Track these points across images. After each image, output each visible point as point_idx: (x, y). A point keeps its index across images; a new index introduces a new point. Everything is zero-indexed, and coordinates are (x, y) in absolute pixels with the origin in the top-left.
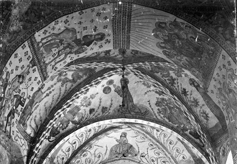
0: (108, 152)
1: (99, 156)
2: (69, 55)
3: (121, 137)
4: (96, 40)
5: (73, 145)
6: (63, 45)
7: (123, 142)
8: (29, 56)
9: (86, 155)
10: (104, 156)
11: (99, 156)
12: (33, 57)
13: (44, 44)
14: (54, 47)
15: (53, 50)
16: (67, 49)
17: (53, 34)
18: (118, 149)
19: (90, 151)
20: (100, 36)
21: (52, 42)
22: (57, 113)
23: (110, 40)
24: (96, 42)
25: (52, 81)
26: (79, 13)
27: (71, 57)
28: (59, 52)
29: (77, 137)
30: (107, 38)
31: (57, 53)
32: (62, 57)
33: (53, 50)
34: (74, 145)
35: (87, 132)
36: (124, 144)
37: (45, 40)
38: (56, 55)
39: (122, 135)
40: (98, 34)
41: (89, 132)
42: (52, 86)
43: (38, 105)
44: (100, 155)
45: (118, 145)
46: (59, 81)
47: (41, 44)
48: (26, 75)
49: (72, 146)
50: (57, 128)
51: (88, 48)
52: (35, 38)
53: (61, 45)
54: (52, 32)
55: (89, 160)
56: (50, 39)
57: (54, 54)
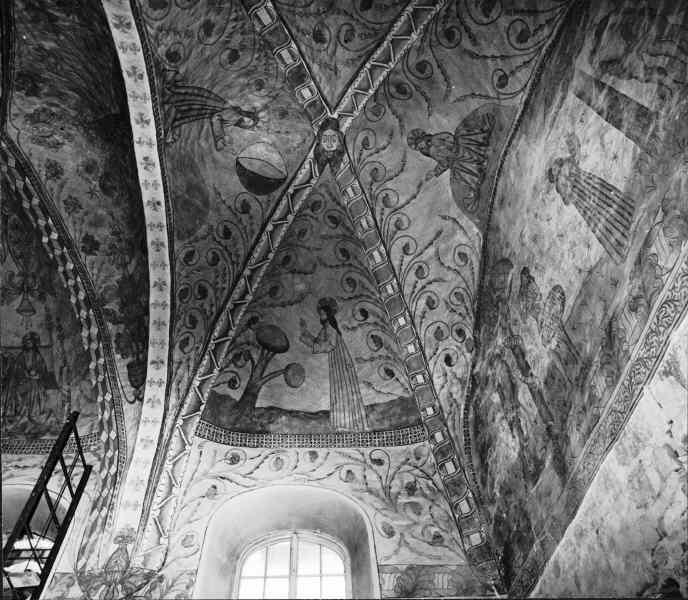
0: (465, 221)
1: (463, 256)
3: (428, 155)
5: (368, 320)
7: (449, 153)
9: (434, 298)
10: (464, 240)
11: (463, 256)
18: (467, 177)
19: (431, 277)
22: (85, 340)
25: (35, 312)
29: (350, 298)
34: (371, 319)
35: (347, 263)
36: (458, 151)
39: (421, 150)
41: (348, 258)
42: (48, 317)
43: (68, 371)
44: (459, 254)
45: (453, 173)
46: (42, 298)
49: (371, 327)
50: (138, 359)
55: (453, 299)
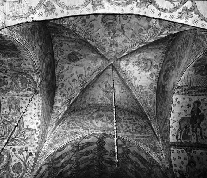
2: (201, 126)
4: (199, 106)
6: (189, 128)
8: (182, 151)
12: (185, 149)
13: (181, 138)
14: (188, 133)
15: (189, 134)
16: (195, 126)
17: (177, 131)
20: (196, 104)
21: (182, 133)
23: (203, 98)
24: (200, 106)
26: (173, 113)
27: (203, 125)
28: (193, 131)
30: (200, 100)
31: (193, 133)
32: (199, 130)
33: (189, 134)
37: (178, 137)
38: (194, 134)
40: (194, 104)
47: (179, 141)
48: (193, 160)
51: (202, 113)
52: (172, 143)
53: (189, 128)
54: (176, 131)
56: (179, 134)
57: (192, 135)
